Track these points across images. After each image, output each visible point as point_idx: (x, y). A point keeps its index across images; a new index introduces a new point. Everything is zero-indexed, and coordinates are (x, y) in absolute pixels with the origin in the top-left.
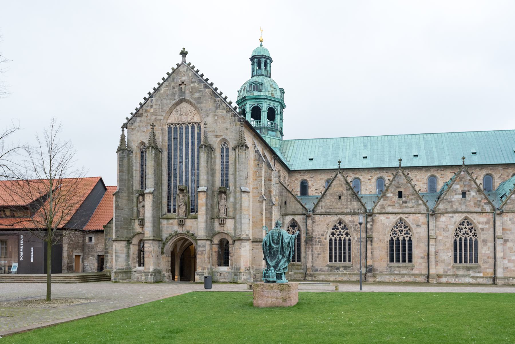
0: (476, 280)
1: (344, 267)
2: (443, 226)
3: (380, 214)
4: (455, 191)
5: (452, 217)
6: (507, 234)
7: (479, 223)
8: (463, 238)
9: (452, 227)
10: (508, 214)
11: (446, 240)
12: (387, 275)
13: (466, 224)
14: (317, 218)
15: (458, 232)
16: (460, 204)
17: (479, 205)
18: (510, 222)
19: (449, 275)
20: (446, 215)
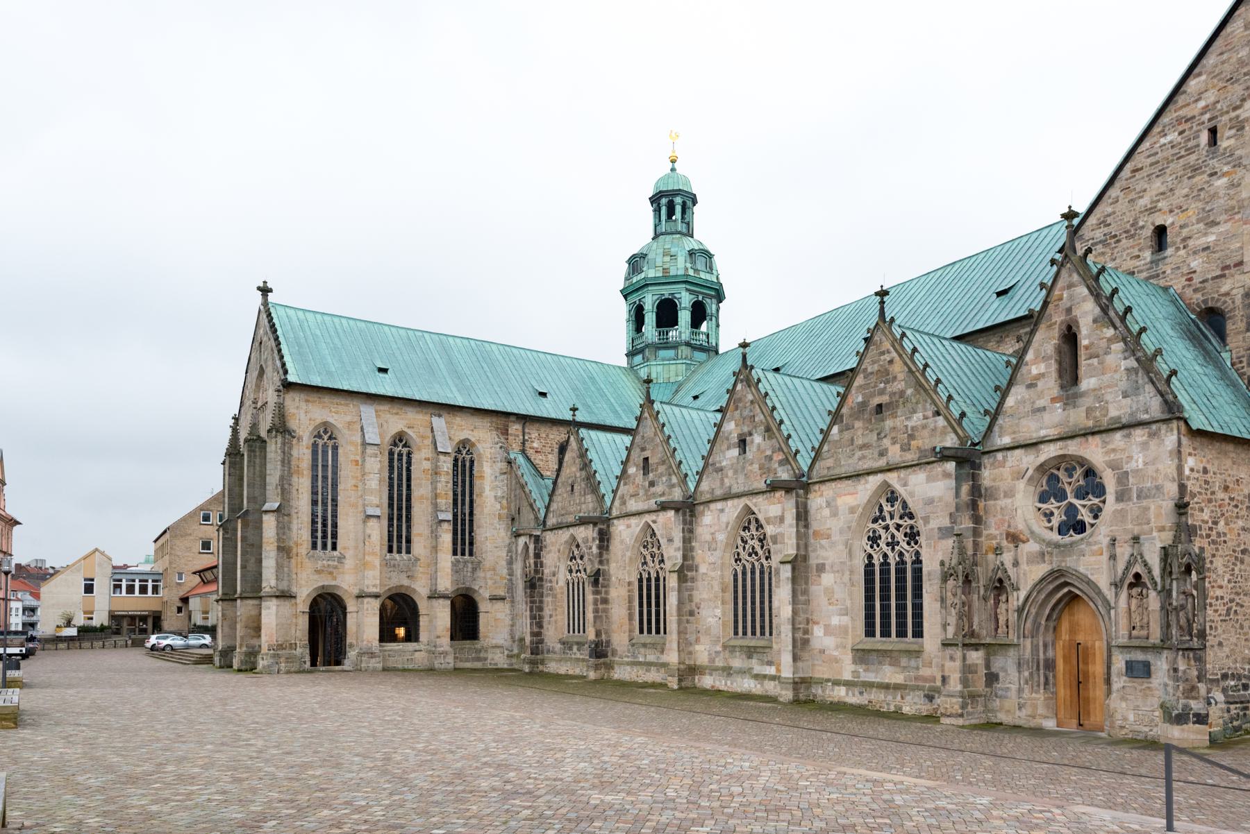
0: (762, 685)
1: (578, 643)
2: (709, 538)
3: (617, 518)
4: (727, 439)
5: (722, 511)
6: (822, 547)
7: (768, 521)
8: (749, 567)
9: (721, 537)
10: (823, 487)
11: (713, 574)
12: (628, 664)
13: (753, 527)
14: (549, 537)
15: (740, 550)
16: (736, 472)
17: (769, 470)
18: (826, 512)
19: (716, 669)
20: (713, 506)
